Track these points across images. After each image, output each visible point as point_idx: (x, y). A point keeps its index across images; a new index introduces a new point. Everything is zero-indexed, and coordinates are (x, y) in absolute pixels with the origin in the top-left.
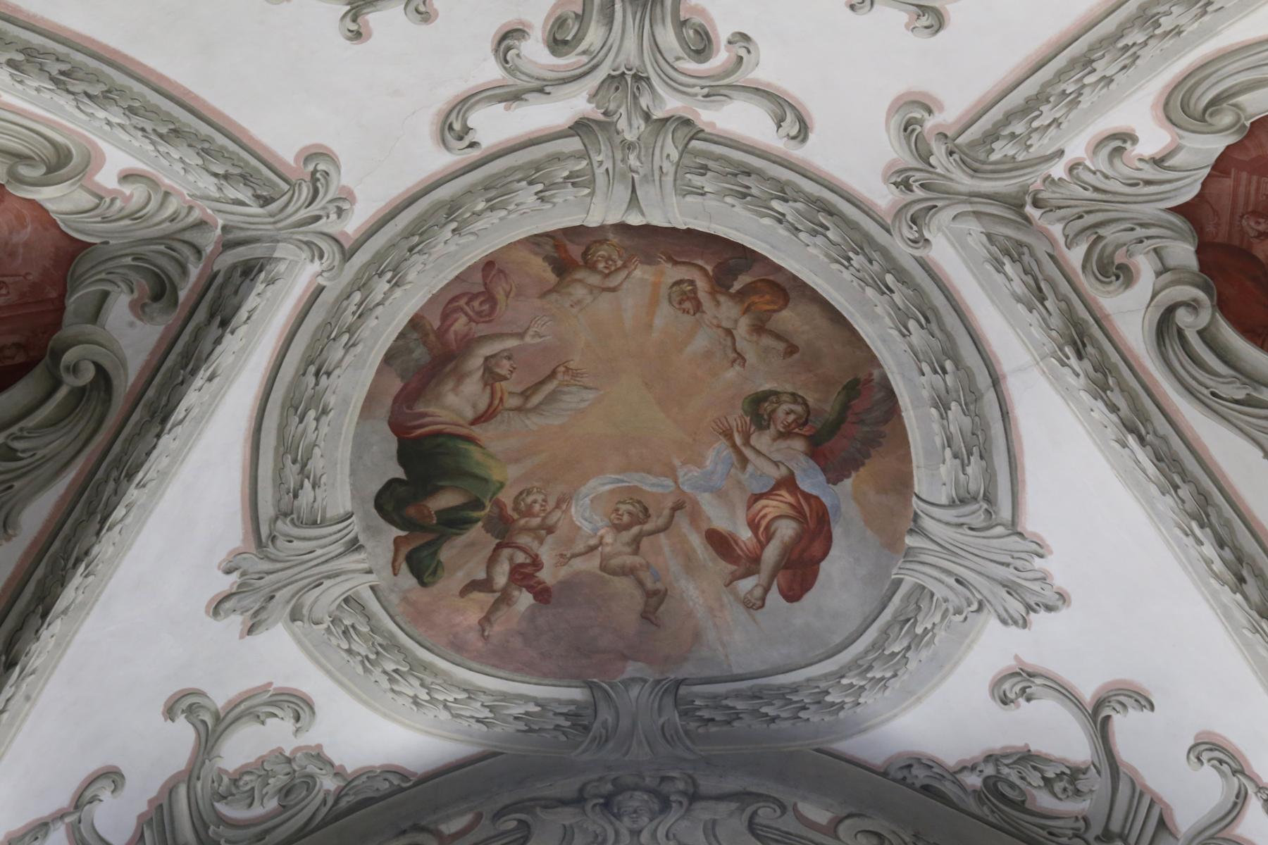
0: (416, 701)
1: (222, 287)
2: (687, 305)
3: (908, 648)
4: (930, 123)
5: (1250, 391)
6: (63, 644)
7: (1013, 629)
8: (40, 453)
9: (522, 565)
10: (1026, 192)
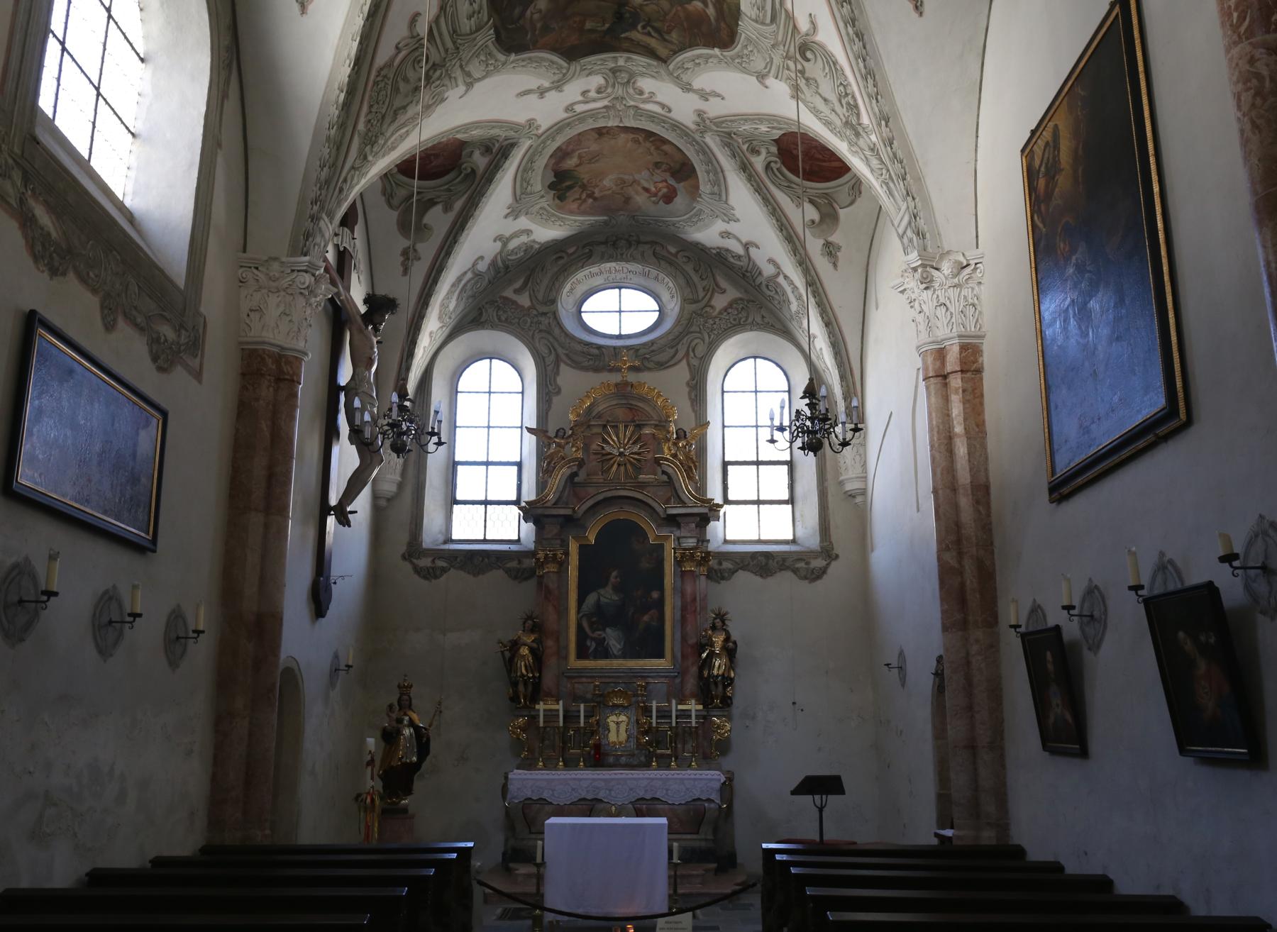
6: (468, 234)
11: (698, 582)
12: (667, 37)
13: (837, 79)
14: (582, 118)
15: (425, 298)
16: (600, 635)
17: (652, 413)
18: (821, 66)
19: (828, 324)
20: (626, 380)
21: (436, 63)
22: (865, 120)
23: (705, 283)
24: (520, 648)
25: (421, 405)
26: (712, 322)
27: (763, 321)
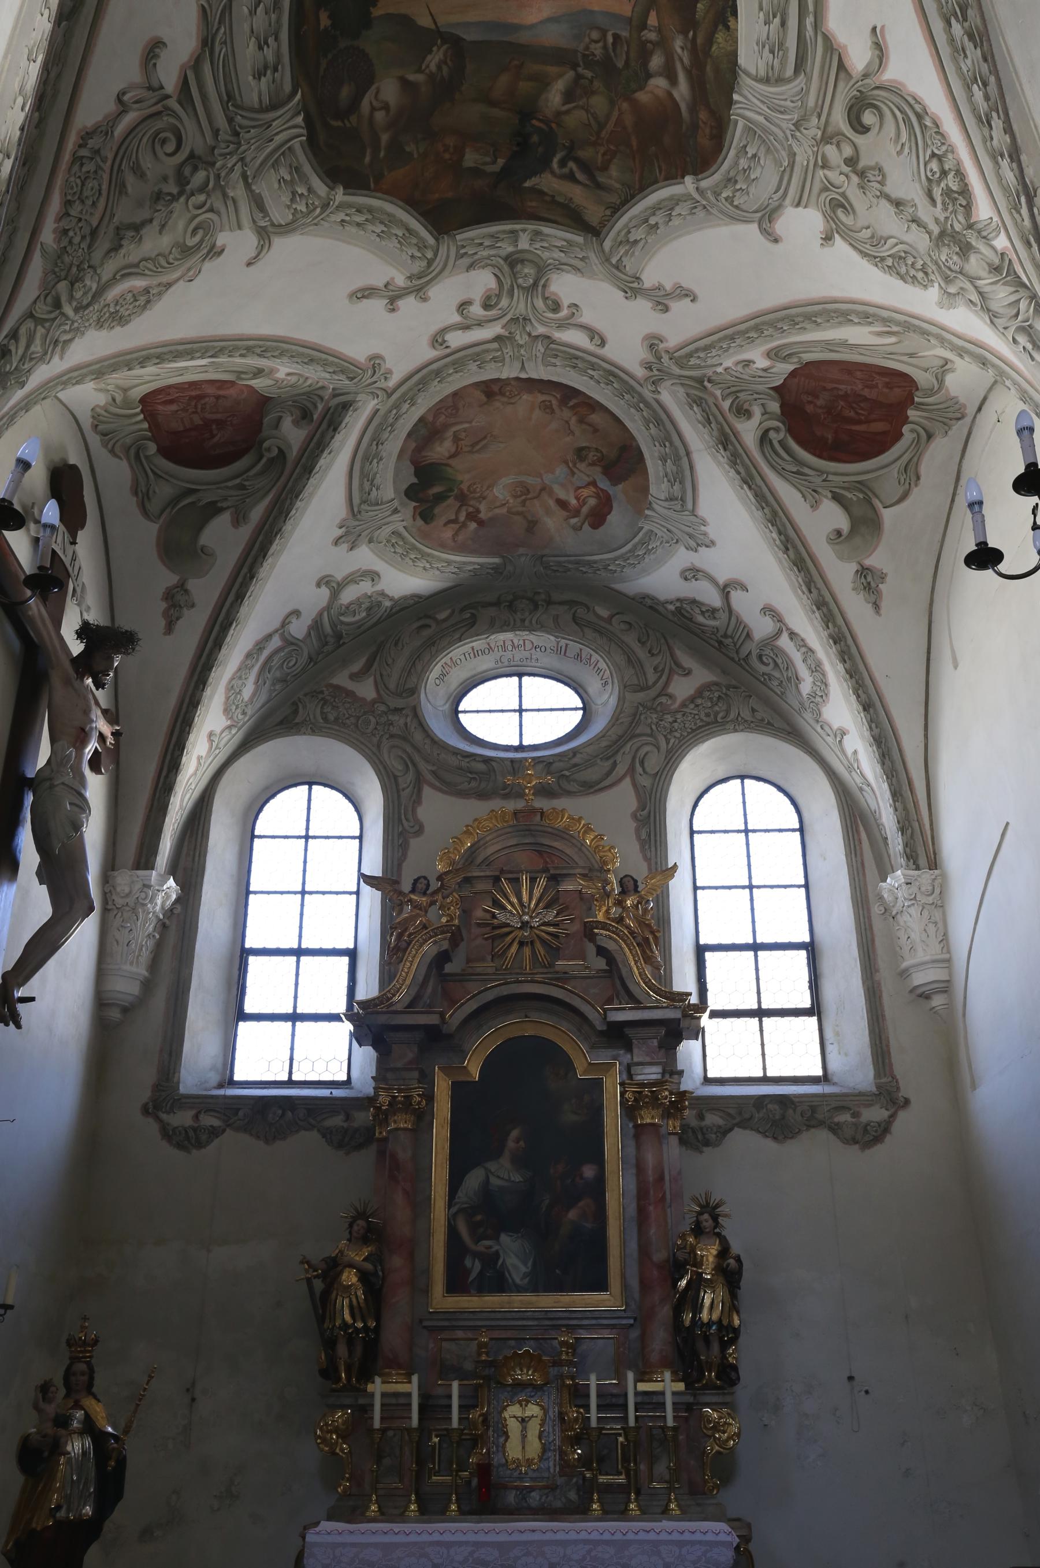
0: (424, 568)
1: (333, 413)
2: (548, 410)
3: (645, 553)
4: (661, 346)
5: (798, 468)
6: (273, 567)
7: (691, 552)
8: (256, 487)
9: (471, 512)
10: (705, 376)
11: (665, 1147)
12: (601, 179)
13: (926, 146)
14: (459, 359)
15: (201, 672)
16: (490, 1247)
17: (576, 858)
18: (892, 134)
19: (867, 707)
20: (531, 806)
21: (197, 153)
22: (984, 210)
23: (657, 660)
24: (341, 1272)
25: (191, 853)
26: (671, 720)
27: (753, 716)
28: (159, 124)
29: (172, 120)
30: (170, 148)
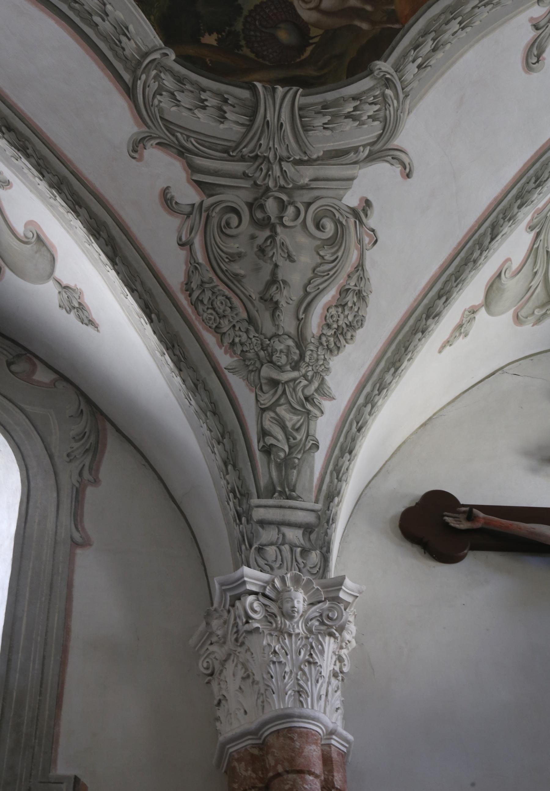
21: (250, 200)
28: (215, 221)
29: (218, 209)
30: (235, 221)
